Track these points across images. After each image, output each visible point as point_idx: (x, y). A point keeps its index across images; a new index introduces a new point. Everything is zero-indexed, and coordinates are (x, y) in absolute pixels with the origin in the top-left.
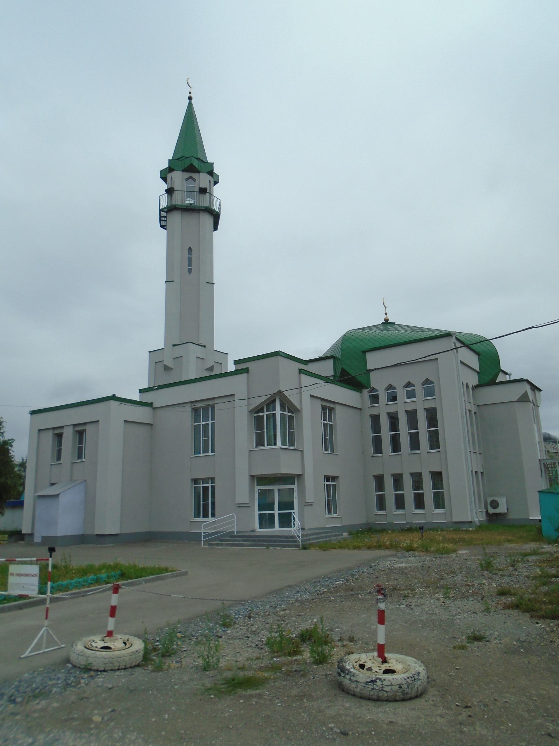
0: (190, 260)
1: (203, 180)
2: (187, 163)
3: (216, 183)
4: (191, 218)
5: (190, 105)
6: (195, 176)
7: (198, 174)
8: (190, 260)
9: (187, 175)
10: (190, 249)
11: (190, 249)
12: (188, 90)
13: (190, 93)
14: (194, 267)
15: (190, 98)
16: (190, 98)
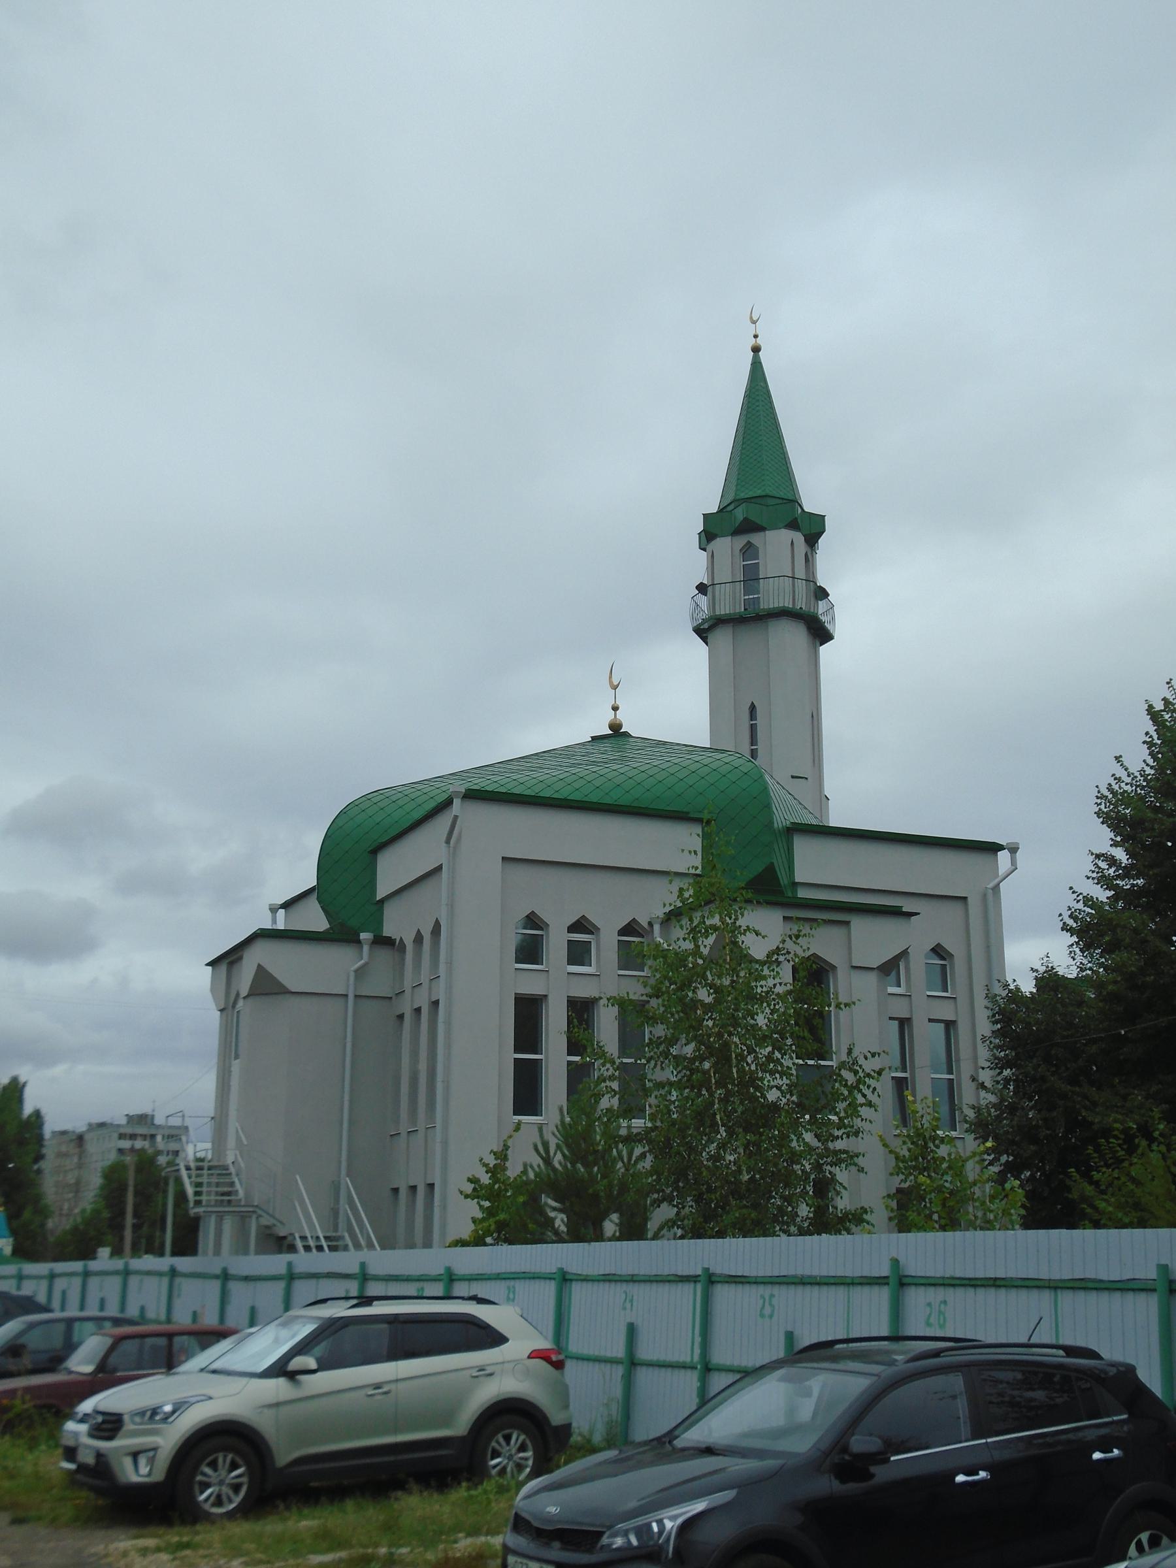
0: (753, 729)
1: (777, 545)
2: (740, 514)
3: (812, 540)
4: (750, 636)
5: (757, 369)
6: (756, 539)
7: (762, 534)
8: (753, 729)
9: (741, 541)
10: (753, 708)
11: (753, 708)
12: (751, 330)
13: (756, 336)
14: (760, 747)
15: (756, 350)
16: (756, 350)
